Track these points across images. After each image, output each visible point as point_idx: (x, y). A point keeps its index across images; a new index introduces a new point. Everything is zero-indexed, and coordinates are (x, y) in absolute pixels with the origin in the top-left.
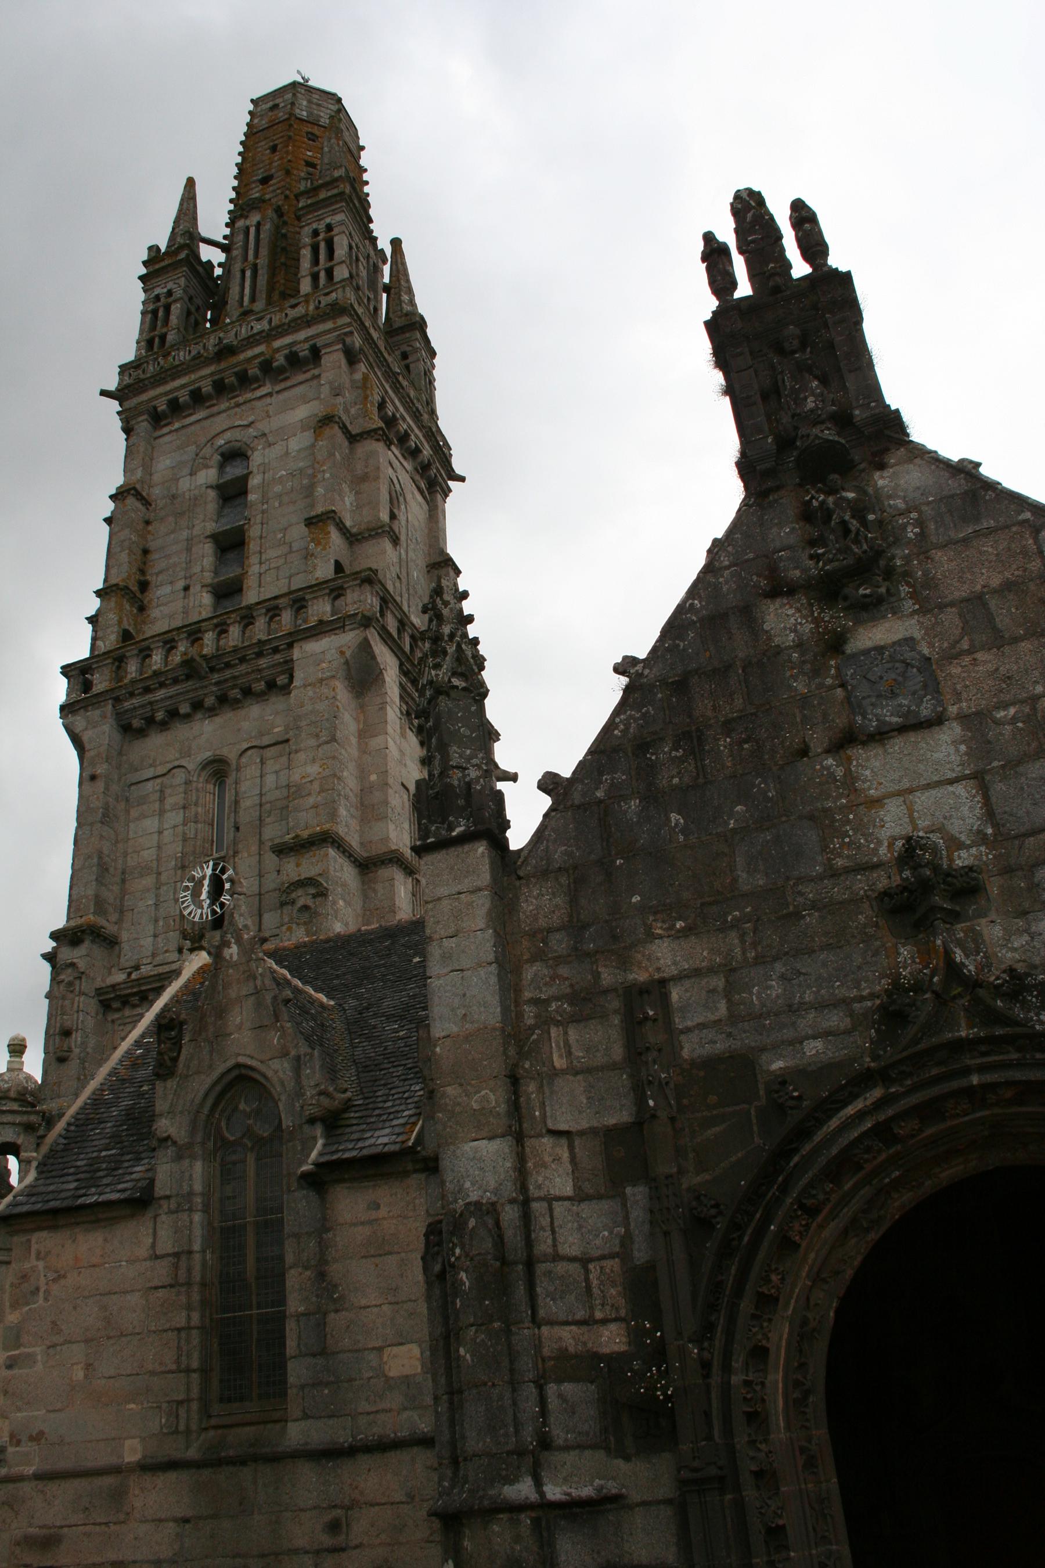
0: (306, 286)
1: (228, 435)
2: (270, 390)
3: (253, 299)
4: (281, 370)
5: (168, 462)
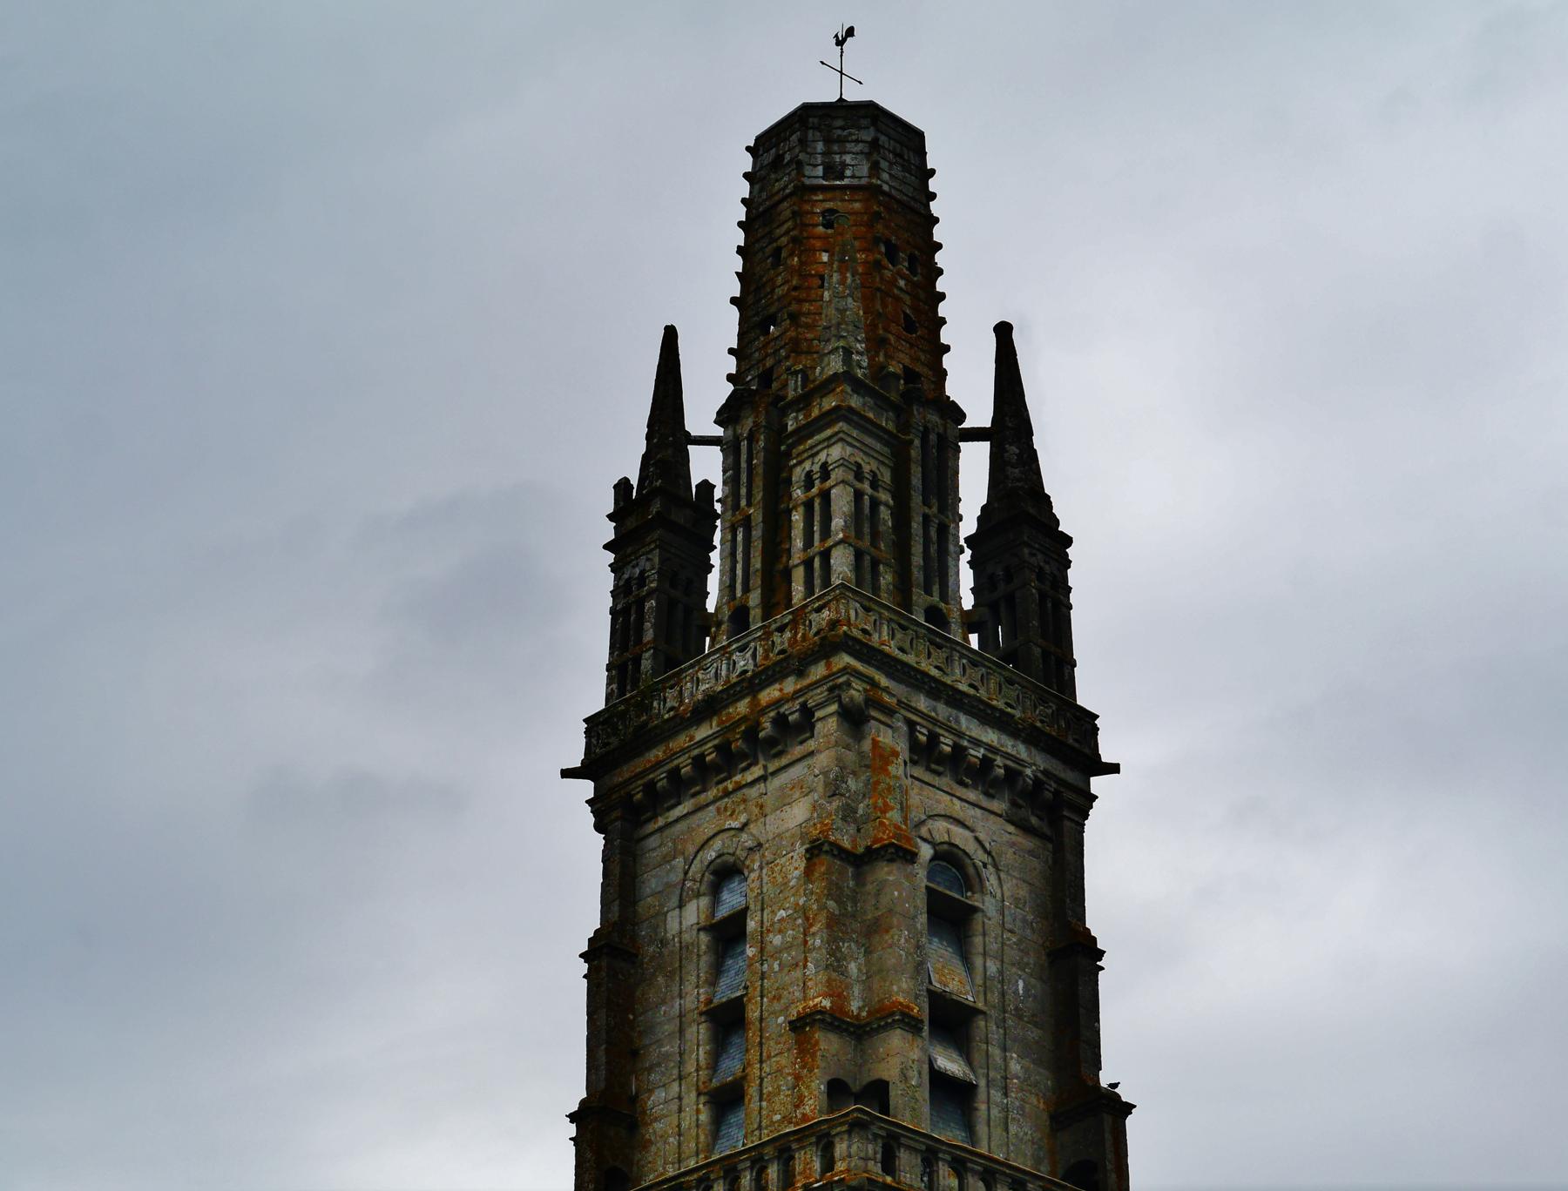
0: (798, 589)
1: (717, 844)
3: (747, 589)
4: (771, 742)
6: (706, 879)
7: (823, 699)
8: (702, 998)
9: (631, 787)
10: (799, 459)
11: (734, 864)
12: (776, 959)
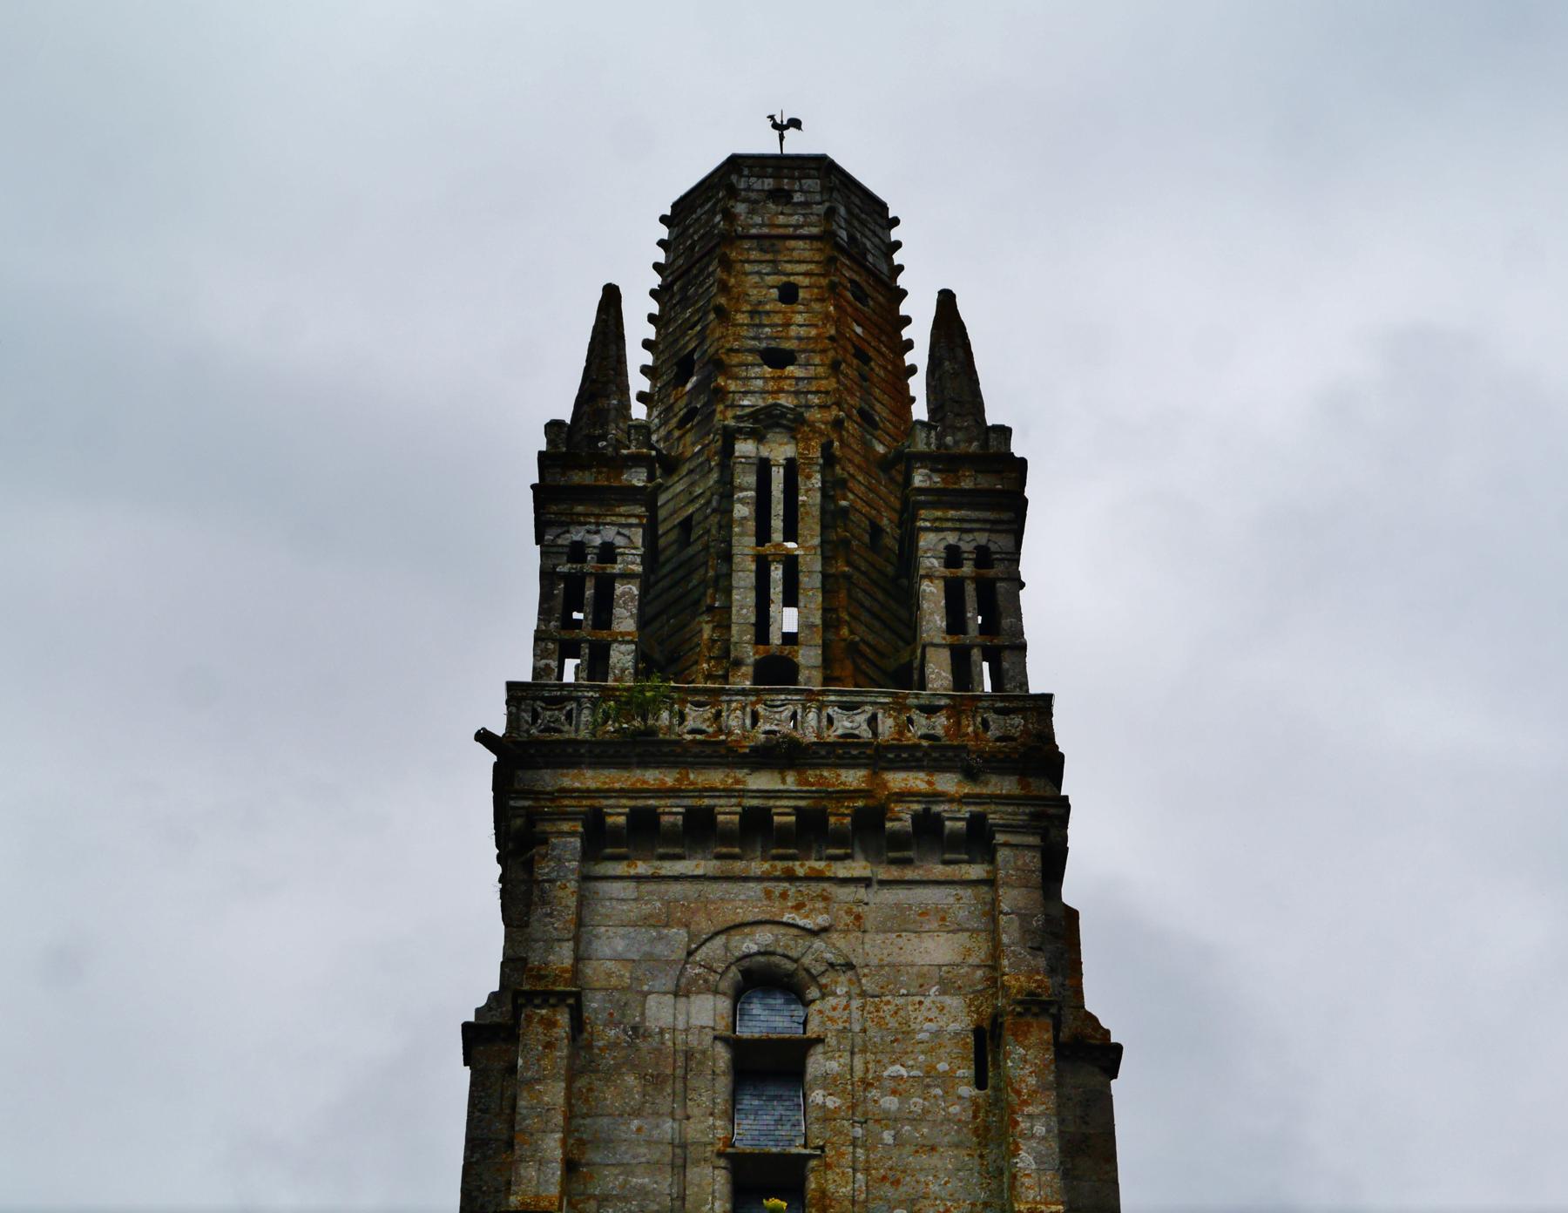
2: (867, 873)
4: (898, 841)
5: (620, 945)
6: (731, 975)
7: (1021, 823)
8: (721, 1134)
9: (605, 802)
10: (937, 524)
11: (791, 975)
12: (887, 1127)
